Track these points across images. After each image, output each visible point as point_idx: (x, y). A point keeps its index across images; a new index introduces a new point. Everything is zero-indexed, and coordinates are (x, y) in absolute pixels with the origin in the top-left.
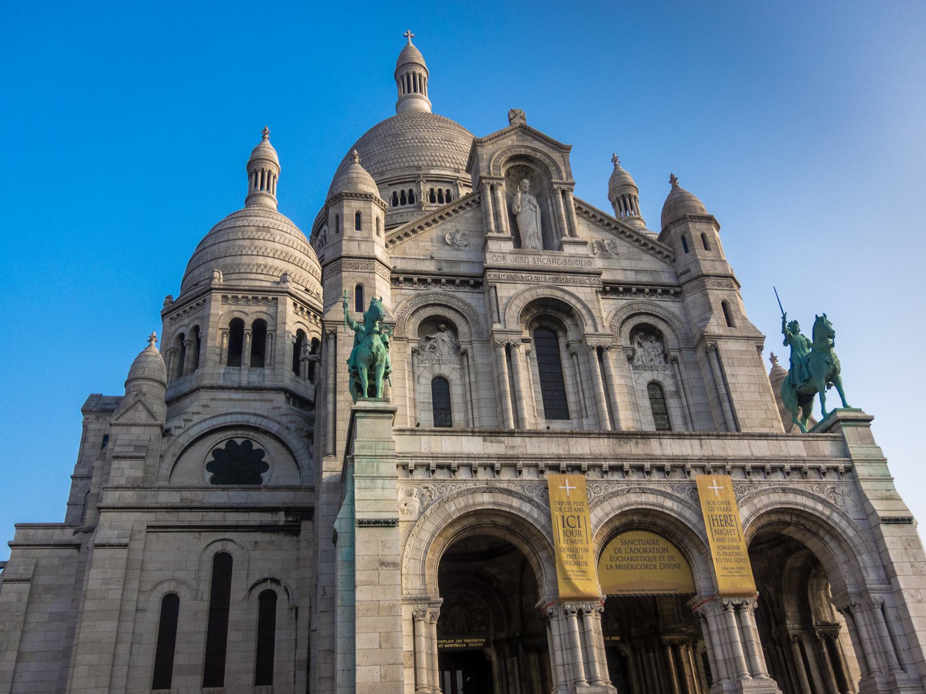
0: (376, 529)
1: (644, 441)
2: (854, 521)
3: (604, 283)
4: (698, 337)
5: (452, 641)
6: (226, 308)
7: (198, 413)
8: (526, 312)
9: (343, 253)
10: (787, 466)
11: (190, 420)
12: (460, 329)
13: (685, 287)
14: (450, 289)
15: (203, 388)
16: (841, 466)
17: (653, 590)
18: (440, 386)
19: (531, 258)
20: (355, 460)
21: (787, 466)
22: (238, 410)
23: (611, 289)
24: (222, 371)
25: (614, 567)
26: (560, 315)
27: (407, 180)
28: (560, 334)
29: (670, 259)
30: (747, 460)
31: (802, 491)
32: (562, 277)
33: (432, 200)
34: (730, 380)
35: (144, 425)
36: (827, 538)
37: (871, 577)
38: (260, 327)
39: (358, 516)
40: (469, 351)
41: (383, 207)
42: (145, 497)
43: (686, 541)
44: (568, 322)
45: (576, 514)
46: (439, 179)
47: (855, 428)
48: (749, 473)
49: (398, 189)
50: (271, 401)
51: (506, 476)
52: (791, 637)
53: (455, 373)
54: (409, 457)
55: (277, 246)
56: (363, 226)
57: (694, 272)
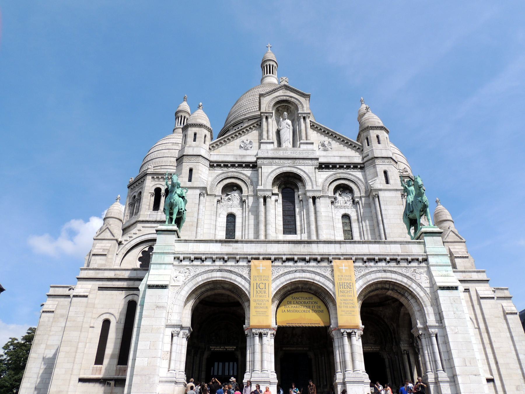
0: (157, 289)
1: (309, 245)
2: (425, 288)
3: (319, 163)
4: (370, 190)
5: (219, 347)
6: (154, 183)
7: (136, 234)
8: (278, 180)
9: (185, 154)
10: (388, 258)
11: (132, 237)
12: (243, 190)
13: (365, 164)
14: (239, 170)
15: (139, 221)
16: (420, 258)
17: (306, 324)
18: (231, 218)
19: (281, 152)
20: (153, 255)
21: (388, 258)
23: (323, 166)
24: (149, 213)
25: (286, 311)
26: (296, 180)
27: (257, 117)
28: (296, 190)
29: (360, 150)
30: (365, 255)
31: (395, 272)
32: (297, 161)
34: (383, 213)
36: (409, 298)
37: (431, 320)
39: (149, 283)
40: (247, 201)
41: (209, 130)
42: (98, 273)
43: (327, 298)
44: (299, 184)
45: (264, 282)
47: (431, 238)
48: (365, 262)
52: (402, 351)
53: (239, 211)
54: (180, 253)
56: (197, 139)
57: (370, 156)
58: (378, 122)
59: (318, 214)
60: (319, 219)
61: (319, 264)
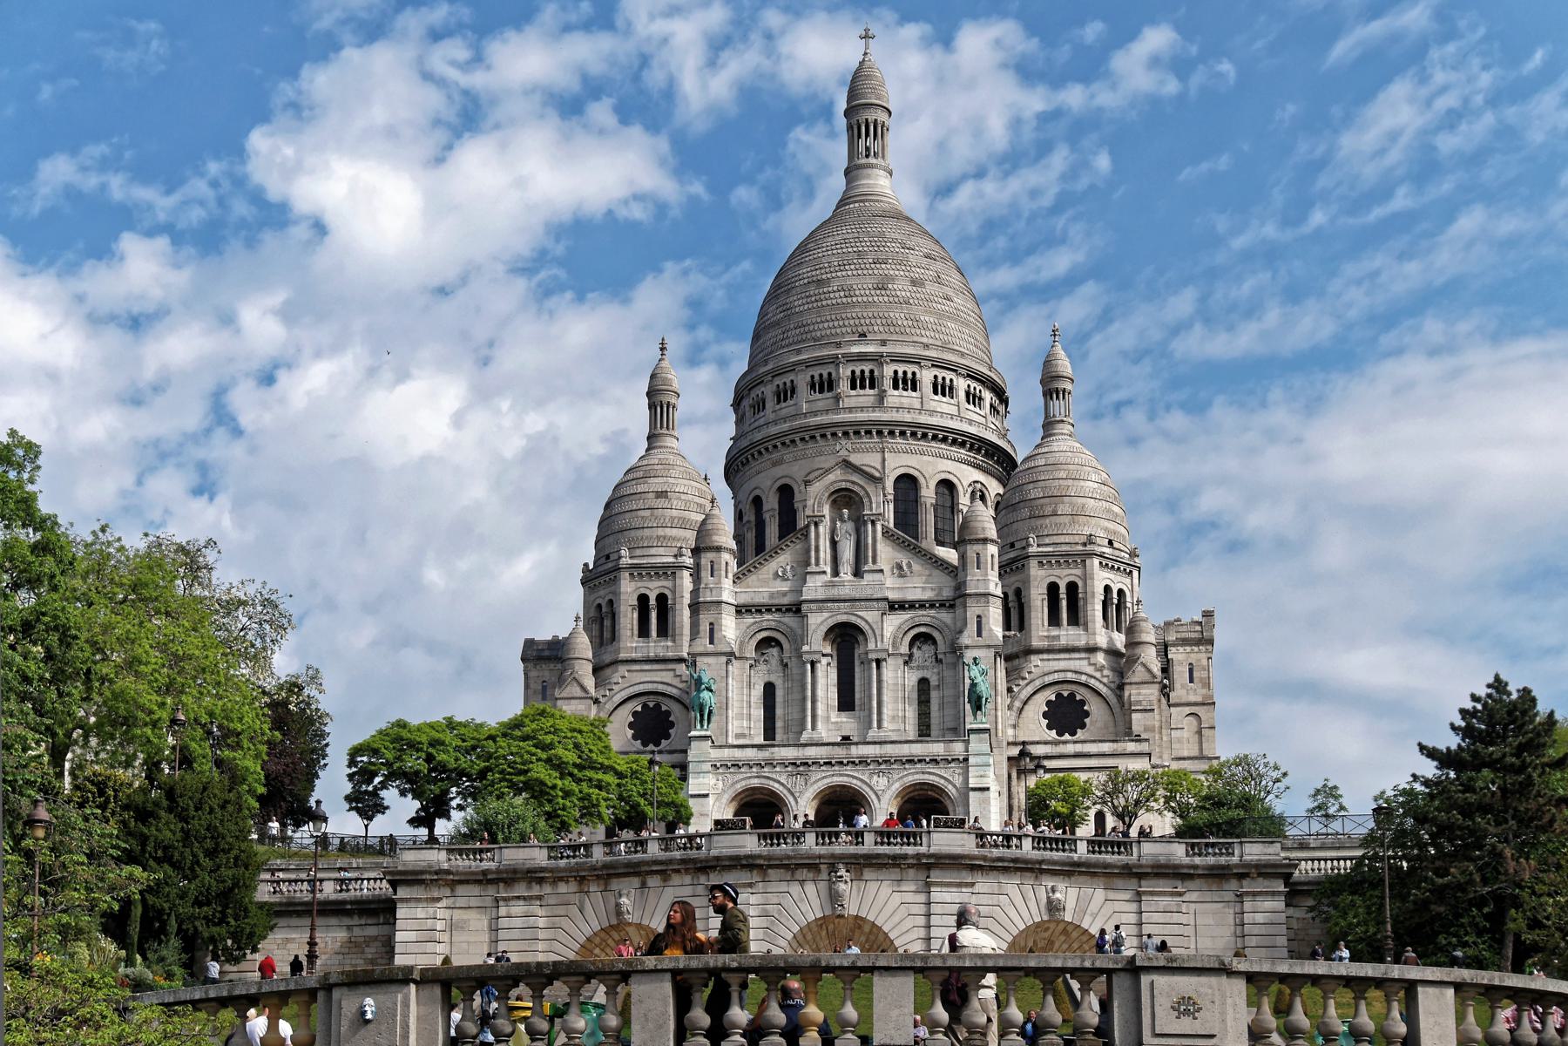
9: (701, 599)
10: (928, 759)
13: (958, 602)
14: (777, 616)
16: (961, 758)
18: (769, 689)
21: (928, 759)
22: (649, 679)
24: (634, 645)
28: (856, 646)
33: (853, 387)
35: (581, 698)
38: (662, 599)
44: (860, 638)
46: (862, 358)
49: (816, 372)
50: (674, 670)
51: (766, 769)
55: (675, 513)
58: (984, 529)
59: (885, 685)
60: (885, 691)
61: (858, 767)
